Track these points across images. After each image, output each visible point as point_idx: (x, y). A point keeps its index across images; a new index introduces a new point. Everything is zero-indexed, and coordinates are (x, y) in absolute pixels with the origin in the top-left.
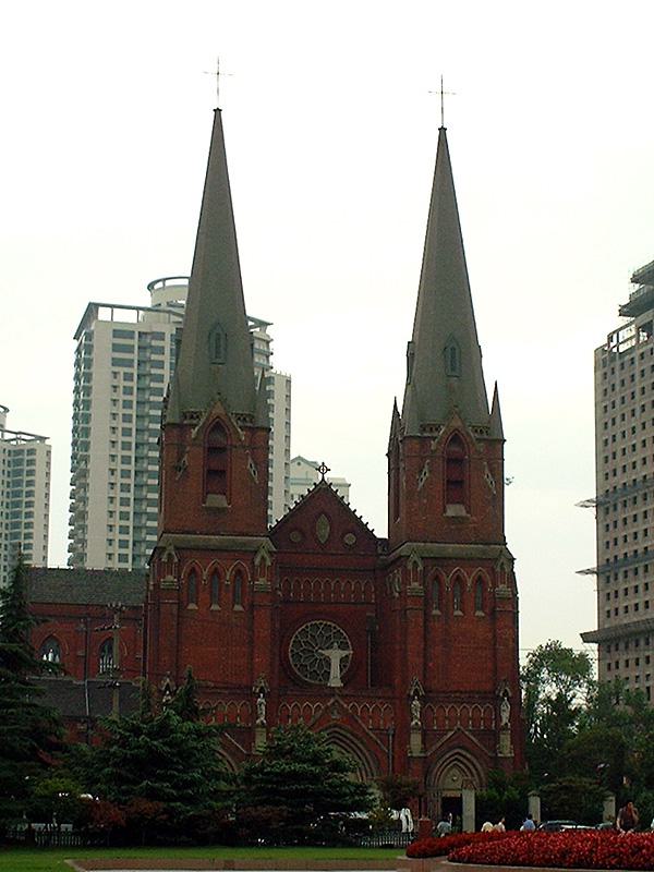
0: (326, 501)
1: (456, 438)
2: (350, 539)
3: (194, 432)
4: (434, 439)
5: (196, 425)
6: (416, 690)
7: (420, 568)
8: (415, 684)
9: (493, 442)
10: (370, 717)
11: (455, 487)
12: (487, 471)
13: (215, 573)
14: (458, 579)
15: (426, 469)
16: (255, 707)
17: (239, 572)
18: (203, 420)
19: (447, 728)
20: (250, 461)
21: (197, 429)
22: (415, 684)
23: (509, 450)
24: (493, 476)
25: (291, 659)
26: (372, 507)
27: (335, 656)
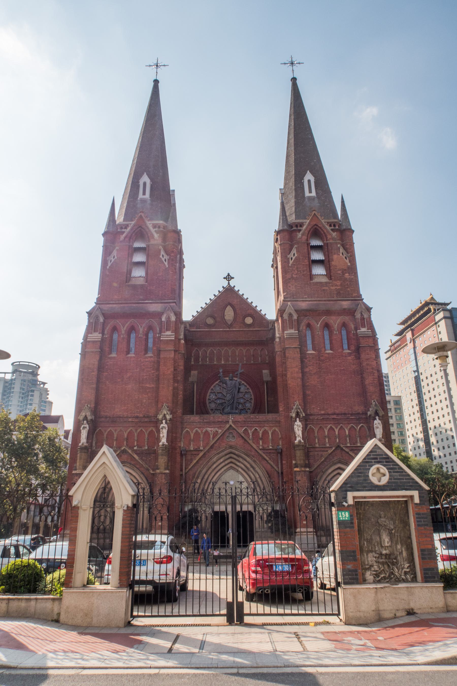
0: (229, 297)
2: (249, 321)
3: (122, 237)
7: (295, 317)
8: (297, 405)
13: (132, 329)
14: (327, 326)
16: (159, 432)
19: (328, 445)
22: (297, 405)
23: (356, 237)
24: (348, 253)
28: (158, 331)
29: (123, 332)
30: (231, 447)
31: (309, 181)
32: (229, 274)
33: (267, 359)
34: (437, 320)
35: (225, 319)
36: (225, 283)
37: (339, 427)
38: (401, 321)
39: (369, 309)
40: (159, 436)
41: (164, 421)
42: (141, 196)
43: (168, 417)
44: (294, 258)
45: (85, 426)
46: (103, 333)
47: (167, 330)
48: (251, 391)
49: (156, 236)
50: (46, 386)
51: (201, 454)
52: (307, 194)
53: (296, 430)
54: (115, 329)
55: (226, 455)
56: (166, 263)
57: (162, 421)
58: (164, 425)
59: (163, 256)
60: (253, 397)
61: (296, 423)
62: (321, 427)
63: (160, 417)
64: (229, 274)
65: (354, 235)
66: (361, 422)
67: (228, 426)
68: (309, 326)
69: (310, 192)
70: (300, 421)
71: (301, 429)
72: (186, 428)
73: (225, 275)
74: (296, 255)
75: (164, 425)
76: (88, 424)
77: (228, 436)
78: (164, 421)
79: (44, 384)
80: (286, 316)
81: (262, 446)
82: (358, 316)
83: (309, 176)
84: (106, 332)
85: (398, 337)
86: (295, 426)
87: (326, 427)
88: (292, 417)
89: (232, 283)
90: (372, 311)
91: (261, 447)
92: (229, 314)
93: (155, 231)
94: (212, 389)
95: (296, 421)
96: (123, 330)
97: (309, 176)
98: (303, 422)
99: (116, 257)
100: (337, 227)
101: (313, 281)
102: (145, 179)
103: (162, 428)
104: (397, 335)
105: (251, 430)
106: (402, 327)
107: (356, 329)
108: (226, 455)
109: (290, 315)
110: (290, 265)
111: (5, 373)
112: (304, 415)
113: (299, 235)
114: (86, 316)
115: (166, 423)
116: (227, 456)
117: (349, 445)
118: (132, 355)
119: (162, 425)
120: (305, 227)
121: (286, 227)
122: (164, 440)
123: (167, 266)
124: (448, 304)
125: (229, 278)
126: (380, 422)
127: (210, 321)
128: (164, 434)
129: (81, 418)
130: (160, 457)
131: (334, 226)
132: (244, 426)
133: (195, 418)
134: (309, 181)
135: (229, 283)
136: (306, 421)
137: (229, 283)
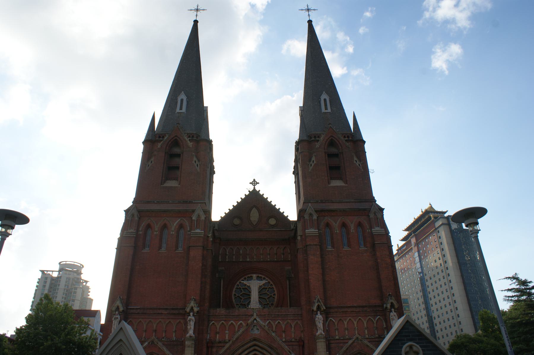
1: (332, 143)
2: (272, 222)
4: (318, 141)
5: (161, 141)
6: (318, 306)
7: (315, 217)
9: (356, 141)
10: (284, 332)
11: (335, 170)
12: (355, 159)
13: (165, 226)
14: (344, 225)
15: (313, 159)
16: (186, 324)
17: (181, 226)
18: (166, 138)
19: (347, 337)
20: (195, 159)
21: (162, 142)
24: (360, 161)
25: (234, 300)
26: (285, 199)
27: (255, 286)
28: (189, 229)
29: (156, 229)
30: (255, 340)
31: (325, 100)
32: (254, 180)
33: (289, 257)
34: (437, 226)
35: (250, 221)
36: (251, 188)
37: (357, 319)
38: (406, 228)
39: (382, 210)
40: (186, 328)
41: (191, 314)
42: (178, 110)
43: (196, 309)
44: (313, 165)
45: (117, 316)
46: (138, 230)
47: (197, 228)
48: (274, 286)
49: (190, 144)
50: (88, 284)
51: (227, 345)
52: (323, 110)
53: (317, 323)
54: (149, 226)
55: (250, 347)
56: (198, 169)
57: (189, 313)
58: (191, 317)
59: (195, 162)
60: (276, 292)
61: (317, 316)
62: (340, 319)
63: (188, 310)
64: (254, 180)
65: (365, 145)
66: (378, 314)
67: (252, 319)
68: (328, 225)
69: (326, 109)
70: (321, 314)
71: (321, 322)
72: (212, 321)
73: (252, 181)
74: (315, 162)
75: (191, 317)
76: (120, 315)
77: (252, 329)
78: (191, 314)
79: (86, 282)
80: (306, 217)
81: (285, 338)
82: (372, 216)
83: (324, 96)
84: (140, 229)
85: (404, 242)
86: (316, 319)
87: (346, 320)
88: (313, 310)
89: (257, 188)
90: (384, 211)
91: (284, 340)
92: (255, 216)
93: (189, 140)
94: (238, 285)
95: (317, 314)
96: (157, 227)
97: (324, 96)
98: (323, 315)
99: (153, 162)
100: (350, 139)
101: (331, 185)
102: (183, 96)
103: (190, 321)
104: (402, 240)
105: (274, 323)
106: (406, 233)
107: (371, 228)
108: (250, 347)
109: (311, 215)
110: (310, 171)
111: (53, 271)
112: (325, 308)
113: (317, 145)
114: (123, 214)
115: (193, 315)
116: (252, 349)
117: (367, 336)
118: (163, 250)
119: (189, 317)
120: (321, 138)
121: (305, 138)
122: (191, 332)
123: (199, 171)
124: (445, 213)
125: (254, 183)
126: (395, 314)
127: (237, 222)
128: (191, 326)
129: (114, 309)
130: (186, 349)
131: (348, 137)
132: (268, 320)
133: (222, 311)
134: (325, 100)
135: (254, 188)
136: (327, 314)
137: (254, 188)
